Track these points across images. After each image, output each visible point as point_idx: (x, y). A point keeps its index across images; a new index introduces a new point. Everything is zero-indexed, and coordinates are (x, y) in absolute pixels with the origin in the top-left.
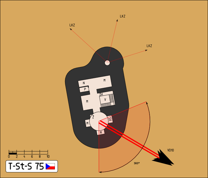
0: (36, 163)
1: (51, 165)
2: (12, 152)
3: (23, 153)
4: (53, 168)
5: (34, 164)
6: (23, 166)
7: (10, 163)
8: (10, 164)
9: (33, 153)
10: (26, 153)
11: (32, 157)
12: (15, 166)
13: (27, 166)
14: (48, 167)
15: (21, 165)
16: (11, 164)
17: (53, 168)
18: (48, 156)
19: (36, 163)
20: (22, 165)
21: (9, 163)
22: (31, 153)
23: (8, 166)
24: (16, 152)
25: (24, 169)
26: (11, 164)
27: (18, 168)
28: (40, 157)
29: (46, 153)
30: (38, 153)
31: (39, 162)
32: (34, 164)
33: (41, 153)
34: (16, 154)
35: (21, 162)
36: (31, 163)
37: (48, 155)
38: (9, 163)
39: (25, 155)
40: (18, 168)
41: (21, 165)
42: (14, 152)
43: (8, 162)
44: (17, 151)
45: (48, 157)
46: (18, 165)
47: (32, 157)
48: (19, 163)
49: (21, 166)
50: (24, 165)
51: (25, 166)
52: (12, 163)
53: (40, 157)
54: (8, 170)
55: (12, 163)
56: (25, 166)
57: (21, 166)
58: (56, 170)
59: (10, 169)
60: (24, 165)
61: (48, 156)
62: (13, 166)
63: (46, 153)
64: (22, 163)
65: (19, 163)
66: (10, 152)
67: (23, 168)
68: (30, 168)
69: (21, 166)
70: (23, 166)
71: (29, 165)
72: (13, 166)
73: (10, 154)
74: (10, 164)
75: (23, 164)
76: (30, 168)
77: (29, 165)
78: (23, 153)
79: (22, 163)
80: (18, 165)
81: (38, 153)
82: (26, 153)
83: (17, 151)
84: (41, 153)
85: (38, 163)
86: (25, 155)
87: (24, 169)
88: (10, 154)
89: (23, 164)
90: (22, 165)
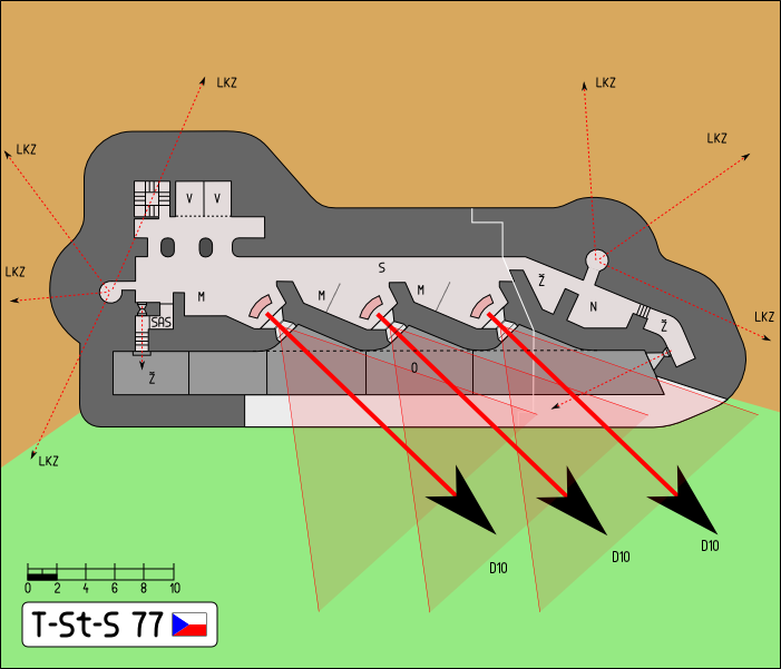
0: (134, 613)
1: (190, 620)
2: (39, 572)
3: (81, 575)
4: (200, 630)
5: (126, 621)
6: (87, 622)
7: (39, 614)
8: (36, 617)
9: (120, 575)
10: (91, 575)
11: (114, 590)
12: (55, 624)
13: (100, 624)
14: (179, 627)
15: (78, 619)
16: (42, 617)
17: (200, 630)
18: (175, 588)
19: (134, 613)
20: (83, 618)
21: (34, 613)
22: (110, 575)
23: (31, 621)
24: (54, 572)
25: (89, 636)
26: (42, 617)
27: (68, 630)
28: (144, 589)
29: (169, 575)
30: (139, 575)
31: (147, 608)
32: (126, 621)
33: (149, 575)
34: (53, 577)
35: (78, 610)
36: (117, 613)
37: (174, 582)
38: (34, 613)
39: (89, 584)
40: (68, 630)
41: (78, 619)
42: (45, 572)
43: (29, 609)
44: (57, 569)
45: (174, 590)
46: (66, 619)
47: (114, 590)
48: (72, 613)
49: (80, 622)
50: (89, 619)
51: (95, 624)
52: (44, 613)
53: (144, 589)
54: (30, 637)
55: (44, 613)
56: (95, 624)
57: (78, 625)
58: (209, 639)
59: (39, 635)
60: (89, 619)
61: (175, 588)
62: (50, 624)
63: (169, 575)
64: (84, 613)
65: (72, 613)
66: (31, 572)
67: (87, 632)
68: (112, 630)
69: (80, 622)
70: (87, 622)
71: (110, 619)
72: (50, 624)
73: (31, 577)
74: (36, 617)
75: (87, 616)
76: (112, 630)
77: (110, 619)
78: (81, 575)
79: (84, 613)
80: (66, 619)
81: (139, 575)
82: (91, 575)
83: (57, 569)
84: (149, 575)
85: (143, 614)
86: (89, 584)
87: (89, 636)
88: (31, 577)
89: (87, 616)
90: (83, 618)
